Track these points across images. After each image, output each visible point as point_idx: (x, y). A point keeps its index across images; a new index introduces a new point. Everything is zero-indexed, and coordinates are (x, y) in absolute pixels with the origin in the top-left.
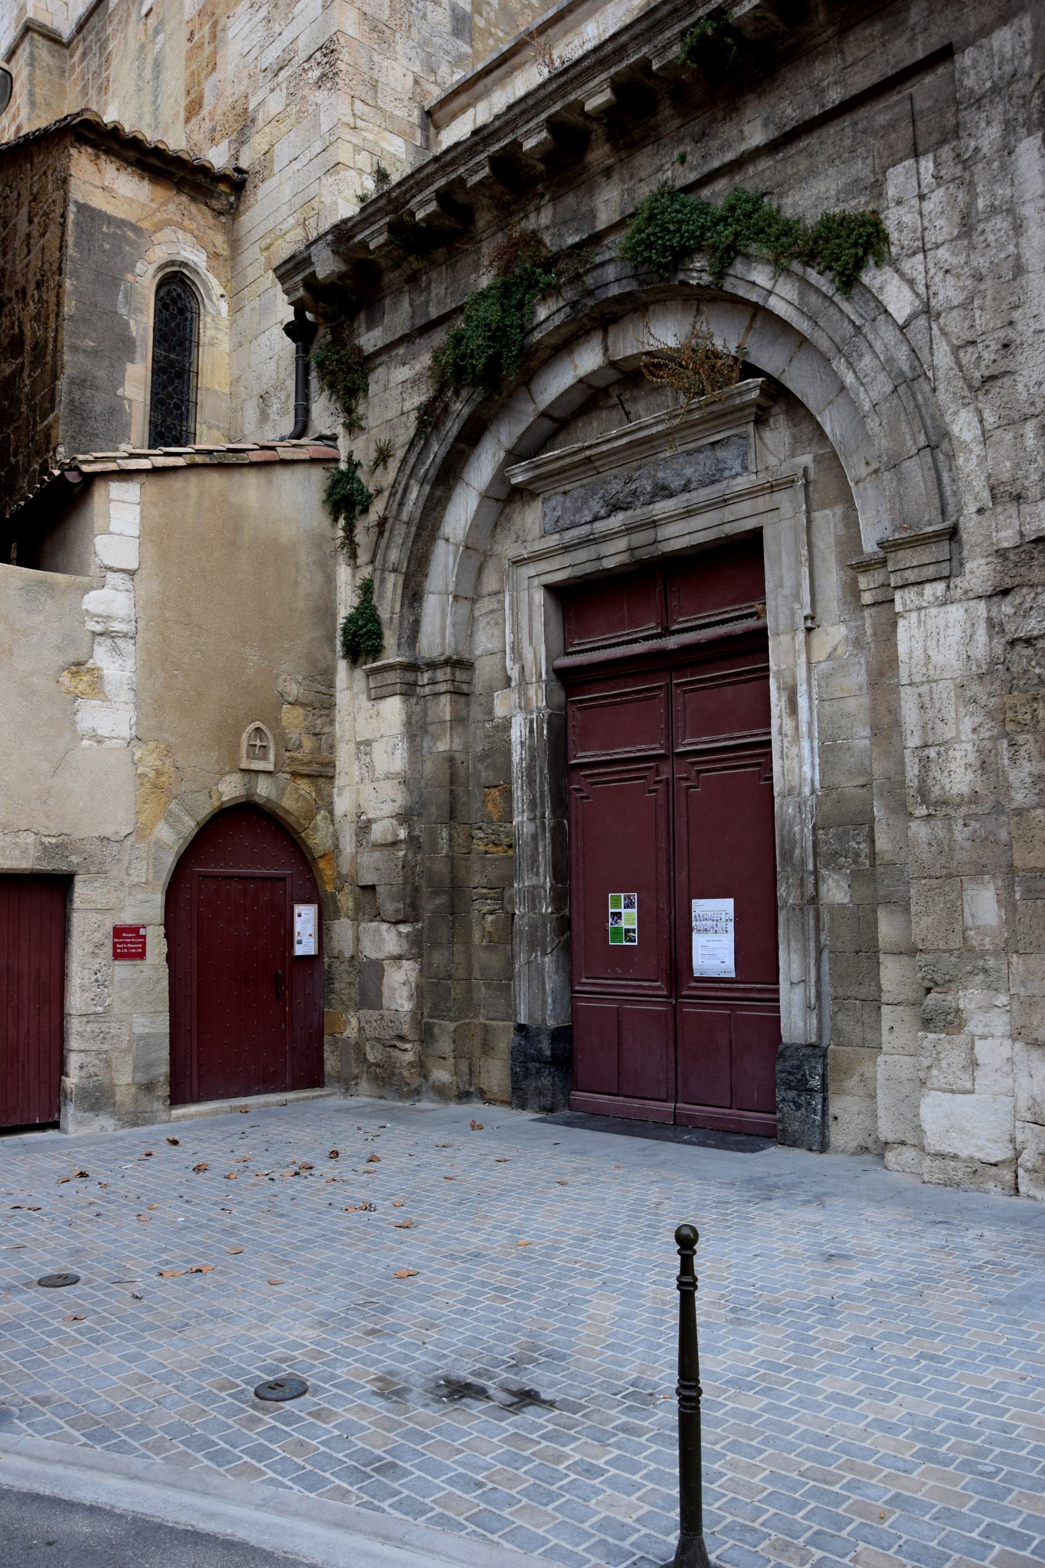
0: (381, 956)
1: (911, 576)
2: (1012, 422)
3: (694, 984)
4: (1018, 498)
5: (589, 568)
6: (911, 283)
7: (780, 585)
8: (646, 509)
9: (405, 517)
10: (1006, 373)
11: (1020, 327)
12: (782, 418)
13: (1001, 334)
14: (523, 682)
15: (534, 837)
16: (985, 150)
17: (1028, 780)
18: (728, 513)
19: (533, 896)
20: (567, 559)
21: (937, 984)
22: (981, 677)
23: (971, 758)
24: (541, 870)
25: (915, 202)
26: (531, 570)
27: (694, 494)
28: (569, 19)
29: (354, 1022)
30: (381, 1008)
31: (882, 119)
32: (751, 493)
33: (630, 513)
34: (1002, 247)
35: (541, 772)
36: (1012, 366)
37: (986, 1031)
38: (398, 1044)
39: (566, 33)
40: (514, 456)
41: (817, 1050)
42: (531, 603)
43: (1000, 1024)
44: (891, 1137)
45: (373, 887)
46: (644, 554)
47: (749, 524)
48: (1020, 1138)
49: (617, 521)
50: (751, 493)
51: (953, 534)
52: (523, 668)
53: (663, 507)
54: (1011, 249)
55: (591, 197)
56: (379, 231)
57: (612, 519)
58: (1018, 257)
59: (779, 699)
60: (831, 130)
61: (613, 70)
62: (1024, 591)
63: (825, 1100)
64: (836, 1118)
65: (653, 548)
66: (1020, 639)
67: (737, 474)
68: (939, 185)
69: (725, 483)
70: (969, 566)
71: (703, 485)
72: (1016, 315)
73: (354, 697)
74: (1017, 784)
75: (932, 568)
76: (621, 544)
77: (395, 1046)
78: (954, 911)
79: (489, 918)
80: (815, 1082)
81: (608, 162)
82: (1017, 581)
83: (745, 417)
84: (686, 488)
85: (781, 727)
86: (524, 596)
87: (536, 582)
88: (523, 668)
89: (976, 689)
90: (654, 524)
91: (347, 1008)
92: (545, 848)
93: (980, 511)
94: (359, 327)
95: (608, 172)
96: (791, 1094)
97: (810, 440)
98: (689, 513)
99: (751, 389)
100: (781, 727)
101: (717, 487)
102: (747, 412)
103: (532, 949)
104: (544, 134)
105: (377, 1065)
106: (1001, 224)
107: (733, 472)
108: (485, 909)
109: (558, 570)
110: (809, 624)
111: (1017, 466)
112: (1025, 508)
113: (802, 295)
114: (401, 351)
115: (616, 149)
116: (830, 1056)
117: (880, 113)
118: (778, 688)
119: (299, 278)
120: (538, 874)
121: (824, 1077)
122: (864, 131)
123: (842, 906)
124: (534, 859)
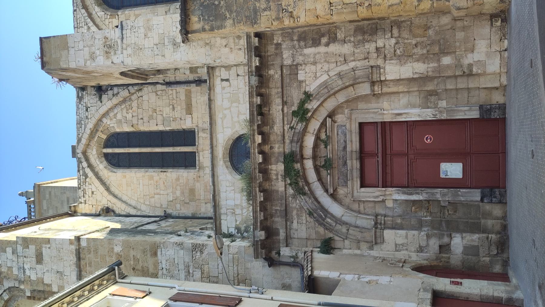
0: (461, 244)
1: (378, 76)
2: (354, 54)
3: (467, 148)
4: (368, 53)
5: (359, 173)
6: (322, 75)
7: (372, 118)
8: (348, 154)
9: (334, 224)
10: (345, 56)
11: (337, 53)
12: (336, 117)
13: (337, 56)
14: (385, 195)
15: (427, 193)
16: (303, 59)
17: (421, 50)
18: (354, 131)
19: (444, 195)
20: (355, 179)
21: (463, 70)
22: (400, 61)
23: (416, 63)
24: (436, 191)
25: (306, 74)
26: (355, 192)
27: (347, 140)
28: (216, 183)
29: (484, 259)
30: (478, 246)
31: (288, 81)
32: (351, 125)
33: (348, 159)
34: (321, 56)
35: (409, 190)
36: (343, 54)
37: (472, 58)
38: (489, 240)
39: (218, 186)
40: (326, 191)
41: (481, 107)
42: (363, 192)
43: (470, 55)
44: (499, 83)
45: (440, 247)
46: (358, 155)
47: (357, 125)
48: (494, 50)
49: (349, 162)
50: (351, 125)
51: (372, 67)
52: (381, 195)
53: (349, 149)
54: (322, 54)
55: (275, 153)
56: (260, 214)
57: (348, 164)
58: (324, 53)
59: (398, 118)
60: (285, 92)
61: (256, 133)
62: (385, 52)
63: (492, 105)
64: (497, 102)
65: (357, 152)
66: (394, 53)
67: (346, 128)
68: (305, 70)
69: (347, 131)
70: (379, 64)
71: (346, 137)
72: (335, 53)
73: (382, 250)
74: (422, 53)
75: (378, 71)
76: (355, 161)
77: (490, 240)
78: (448, 66)
79: (450, 212)
80: (489, 107)
81: (269, 147)
82: (383, 53)
83: (333, 125)
84: (345, 142)
85: (404, 118)
86: (362, 194)
87: (359, 190)
88: (381, 195)
89: (402, 62)
90: (352, 151)
91: (480, 261)
92: (429, 190)
93: (369, 62)
94: (277, 239)
95: (271, 148)
96: (492, 113)
97: (343, 110)
98: (351, 141)
99: (329, 120)
100: (404, 118)
101: (347, 133)
102: (333, 124)
103: (458, 195)
104: (260, 156)
105: (497, 249)
106: (317, 57)
107: (345, 129)
108: (447, 214)
109: (358, 183)
110: (383, 110)
111: (362, 53)
112: (370, 52)
113: (316, 99)
114: (288, 224)
115: (268, 144)
116: (482, 104)
117: (287, 80)
118: (396, 118)
119: (260, 249)
120: (437, 192)
121: (487, 105)
122: (289, 85)
123: (447, 102)
124: (433, 194)
